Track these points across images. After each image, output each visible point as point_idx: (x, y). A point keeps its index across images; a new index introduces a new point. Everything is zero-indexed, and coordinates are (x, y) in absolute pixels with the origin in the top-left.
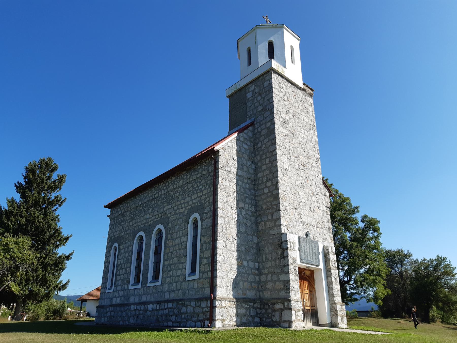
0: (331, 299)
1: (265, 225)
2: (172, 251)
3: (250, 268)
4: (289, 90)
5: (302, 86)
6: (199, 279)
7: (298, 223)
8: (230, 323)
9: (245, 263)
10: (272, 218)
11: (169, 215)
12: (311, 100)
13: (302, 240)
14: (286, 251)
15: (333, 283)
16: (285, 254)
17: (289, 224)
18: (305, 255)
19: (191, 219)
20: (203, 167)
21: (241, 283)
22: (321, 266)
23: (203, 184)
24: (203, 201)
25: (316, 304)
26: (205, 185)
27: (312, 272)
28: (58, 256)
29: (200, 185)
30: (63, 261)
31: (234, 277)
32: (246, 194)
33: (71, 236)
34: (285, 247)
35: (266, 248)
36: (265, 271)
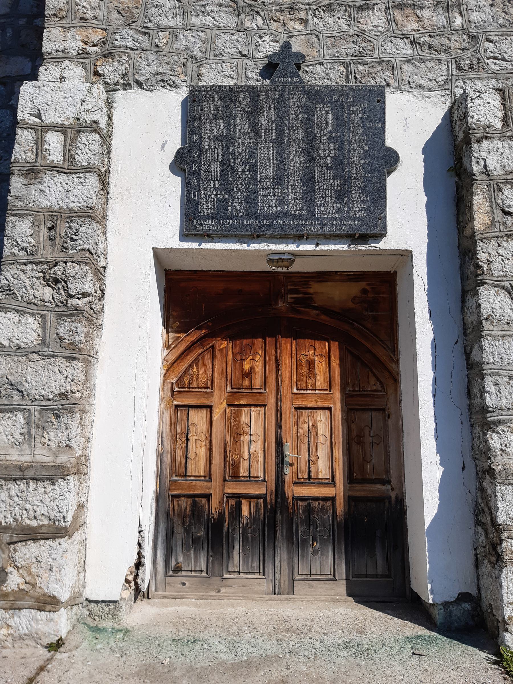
18: (226, 186)
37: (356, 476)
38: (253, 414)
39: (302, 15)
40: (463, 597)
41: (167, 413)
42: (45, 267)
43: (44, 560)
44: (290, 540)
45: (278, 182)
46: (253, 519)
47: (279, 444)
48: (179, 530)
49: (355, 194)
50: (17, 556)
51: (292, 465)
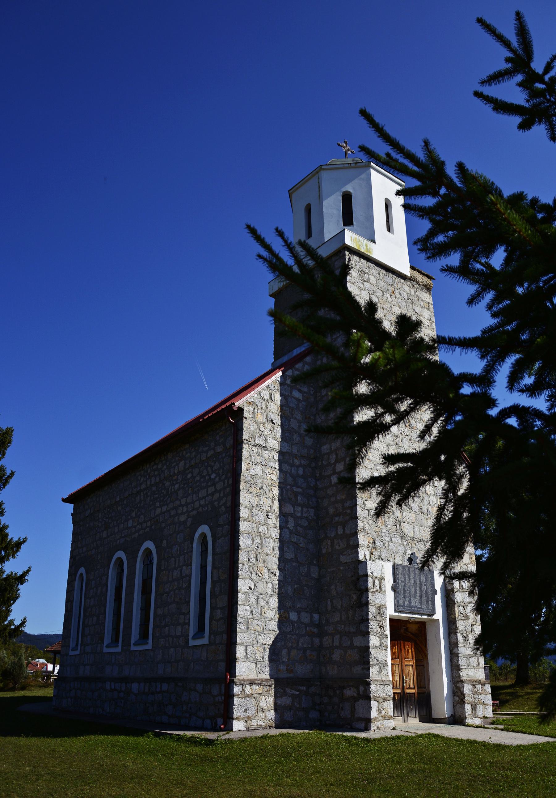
0: (454, 674)
1: (332, 545)
2: (167, 590)
3: (302, 623)
4: (381, 284)
5: (406, 271)
6: (210, 644)
7: (394, 539)
8: (260, 723)
9: (293, 616)
10: (344, 532)
11: (163, 525)
12: (427, 297)
13: (400, 571)
14: (364, 595)
15: (460, 645)
16: (363, 599)
17: (374, 543)
19: (197, 535)
20: (218, 438)
21: (285, 651)
22: (439, 615)
23: (216, 470)
24: (216, 503)
25: (429, 683)
26: (221, 472)
27: (422, 625)
28: (4, 576)
29: (213, 472)
30: (12, 586)
31: (270, 642)
32: (298, 487)
33: (25, 541)
34: (363, 588)
35: (333, 587)
36: (330, 629)
39: (415, 542)
44: (407, 707)
45: (415, 597)
49: (430, 602)
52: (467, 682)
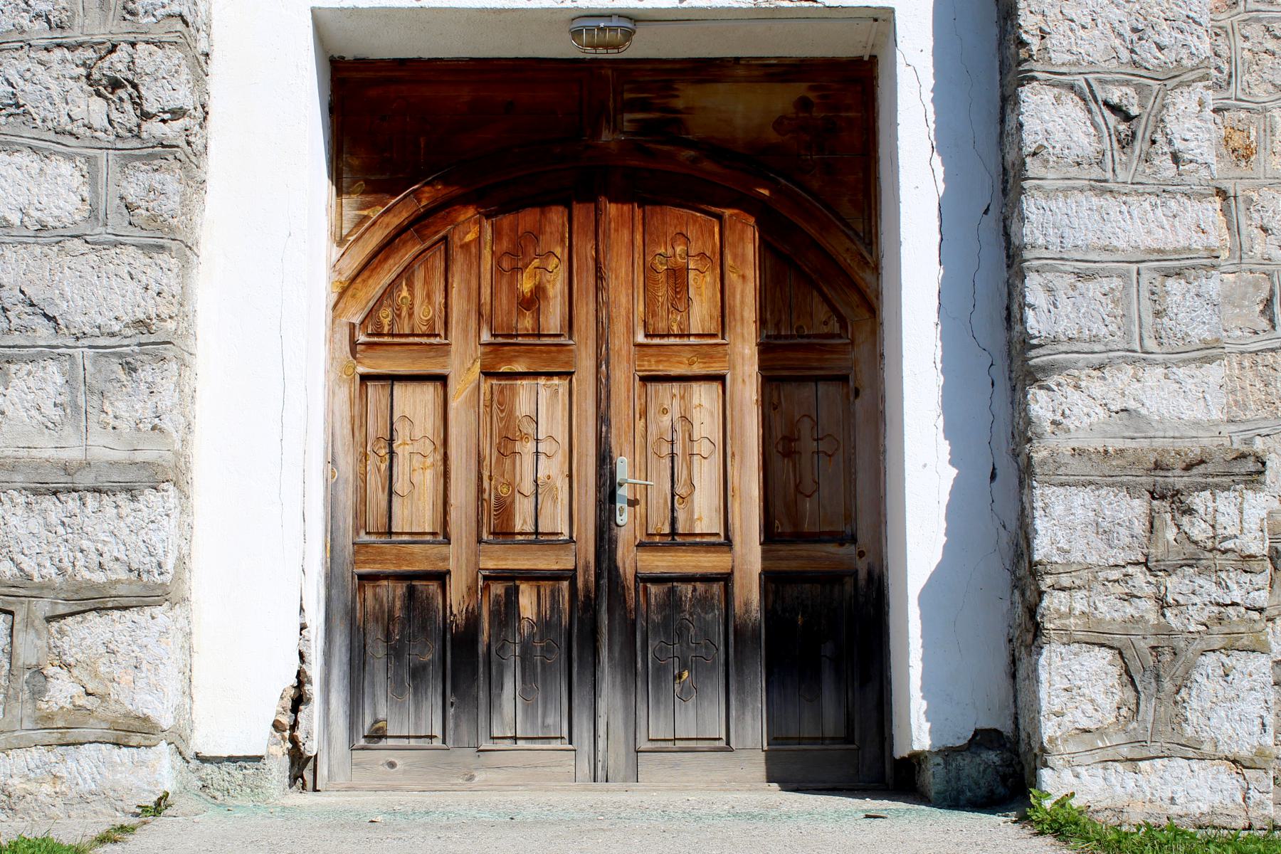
37: (779, 527)
38: (544, 395)
40: (984, 739)
41: (343, 394)
42: (90, 54)
43: (122, 649)
46: (545, 625)
47: (604, 459)
48: (378, 651)
50: (65, 644)
51: (633, 503)
52: (1076, 465)
